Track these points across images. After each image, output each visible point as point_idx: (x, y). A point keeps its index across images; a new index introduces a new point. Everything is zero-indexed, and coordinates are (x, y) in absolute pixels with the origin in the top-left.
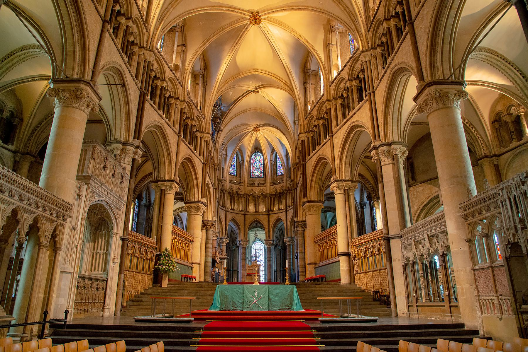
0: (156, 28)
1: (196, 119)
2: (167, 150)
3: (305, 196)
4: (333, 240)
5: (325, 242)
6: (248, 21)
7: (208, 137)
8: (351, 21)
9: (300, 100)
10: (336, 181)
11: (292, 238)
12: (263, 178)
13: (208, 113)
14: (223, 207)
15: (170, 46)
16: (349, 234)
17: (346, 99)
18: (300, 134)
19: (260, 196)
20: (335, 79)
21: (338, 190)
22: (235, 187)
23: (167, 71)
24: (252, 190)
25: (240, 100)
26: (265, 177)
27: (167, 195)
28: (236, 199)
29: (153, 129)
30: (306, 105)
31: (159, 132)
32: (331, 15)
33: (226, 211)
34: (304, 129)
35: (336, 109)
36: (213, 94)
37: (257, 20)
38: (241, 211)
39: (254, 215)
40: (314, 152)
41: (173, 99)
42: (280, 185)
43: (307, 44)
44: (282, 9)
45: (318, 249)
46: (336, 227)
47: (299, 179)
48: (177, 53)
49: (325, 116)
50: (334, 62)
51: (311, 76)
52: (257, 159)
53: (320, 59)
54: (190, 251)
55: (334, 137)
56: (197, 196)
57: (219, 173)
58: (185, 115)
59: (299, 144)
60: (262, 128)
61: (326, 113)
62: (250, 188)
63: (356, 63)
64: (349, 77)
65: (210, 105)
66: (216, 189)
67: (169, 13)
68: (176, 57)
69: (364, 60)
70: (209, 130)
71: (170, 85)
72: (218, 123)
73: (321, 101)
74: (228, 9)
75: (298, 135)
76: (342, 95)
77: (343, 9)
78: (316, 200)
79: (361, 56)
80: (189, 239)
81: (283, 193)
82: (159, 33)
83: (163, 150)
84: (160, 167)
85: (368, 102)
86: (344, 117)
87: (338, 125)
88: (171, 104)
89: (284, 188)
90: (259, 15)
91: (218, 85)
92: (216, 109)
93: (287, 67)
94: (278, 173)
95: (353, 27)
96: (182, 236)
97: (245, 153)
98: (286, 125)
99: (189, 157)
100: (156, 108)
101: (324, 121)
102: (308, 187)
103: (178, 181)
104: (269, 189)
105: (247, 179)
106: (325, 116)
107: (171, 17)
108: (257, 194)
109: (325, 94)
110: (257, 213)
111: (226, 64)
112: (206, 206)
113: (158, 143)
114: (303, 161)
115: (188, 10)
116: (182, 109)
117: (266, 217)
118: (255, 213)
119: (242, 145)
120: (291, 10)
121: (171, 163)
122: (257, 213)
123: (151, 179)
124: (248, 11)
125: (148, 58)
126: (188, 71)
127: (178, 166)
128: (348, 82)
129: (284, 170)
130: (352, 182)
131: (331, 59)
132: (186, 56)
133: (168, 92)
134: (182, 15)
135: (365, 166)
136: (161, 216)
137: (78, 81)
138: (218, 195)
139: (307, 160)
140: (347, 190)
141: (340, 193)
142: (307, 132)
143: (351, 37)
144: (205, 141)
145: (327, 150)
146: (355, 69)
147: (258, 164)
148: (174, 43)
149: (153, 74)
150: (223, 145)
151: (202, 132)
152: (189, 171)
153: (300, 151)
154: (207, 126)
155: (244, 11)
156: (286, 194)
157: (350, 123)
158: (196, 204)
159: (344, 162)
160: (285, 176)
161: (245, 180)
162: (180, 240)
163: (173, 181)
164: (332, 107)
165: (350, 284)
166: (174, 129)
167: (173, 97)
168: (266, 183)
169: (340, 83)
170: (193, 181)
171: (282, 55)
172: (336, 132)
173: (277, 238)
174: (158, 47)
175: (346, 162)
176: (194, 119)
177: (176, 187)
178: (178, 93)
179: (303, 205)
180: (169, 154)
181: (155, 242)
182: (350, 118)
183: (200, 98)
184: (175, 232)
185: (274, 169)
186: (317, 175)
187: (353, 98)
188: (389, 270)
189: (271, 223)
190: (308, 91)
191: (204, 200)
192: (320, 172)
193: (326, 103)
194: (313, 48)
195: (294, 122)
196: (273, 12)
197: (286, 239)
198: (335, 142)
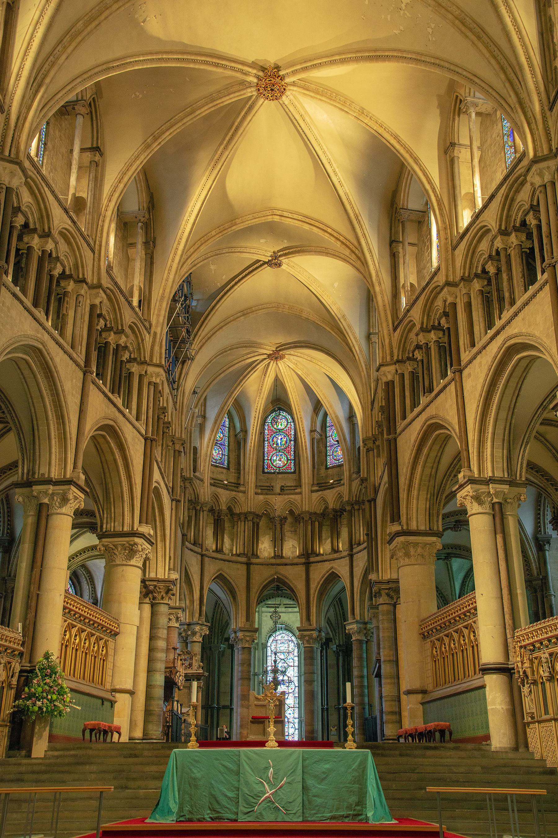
0: (25, 105)
2: (55, 406)
3: (396, 519)
4: (466, 632)
5: (447, 636)
6: (253, 89)
7: (158, 375)
8: (507, 85)
9: (380, 284)
10: (472, 481)
11: (366, 623)
12: (294, 472)
13: (158, 316)
14: (194, 544)
15: (64, 150)
16: (507, 616)
17: (493, 282)
18: (381, 366)
19: (286, 518)
20: (467, 230)
21: (475, 505)
22: (224, 496)
23: (57, 213)
24: (267, 503)
25: (236, 284)
26: (298, 471)
27: (55, 517)
28: (227, 525)
29: (21, 355)
30: (395, 295)
31: (34, 362)
32: (457, 69)
33: (202, 556)
34: (392, 356)
35: (469, 306)
36: (170, 270)
37: (276, 88)
38: (238, 555)
39: (272, 565)
40: (417, 410)
41: (72, 282)
42: (334, 490)
43: (398, 146)
44: (337, 57)
45: (429, 652)
46: (474, 598)
47: (381, 477)
48: (80, 168)
49: (443, 321)
50: (463, 189)
51: (408, 225)
52: (280, 427)
53: (430, 182)
54: (110, 658)
55: (465, 373)
57: (185, 462)
58: (102, 322)
59: (380, 391)
60: (292, 351)
61: (446, 314)
62: (261, 497)
63: (518, 191)
64: (500, 225)
65: (163, 297)
66: (178, 501)
67: (56, 68)
68: (78, 179)
69: (537, 181)
70: (161, 358)
71: (63, 247)
72: (183, 341)
73: (431, 286)
74: (203, 58)
75: (378, 370)
76: (484, 271)
77: (487, 55)
78: (422, 528)
79: (531, 174)
80: (108, 628)
81: (342, 510)
82: (34, 117)
83: (45, 406)
84: (37, 447)
85: (547, 288)
86: (490, 324)
87: (473, 345)
88: (65, 294)
89: (346, 498)
90: (281, 73)
91: (181, 247)
92: (179, 305)
93: (350, 203)
94: (330, 461)
95: (513, 99)
96: (90, 620)
97: (249, 411)
98: (348, 344)
99: (111, 423)
100: (29, 304)
101: (441, 336)
102: (403, 495)
103: (82, 482)
105: (254, 477)
106: (443, 321)
107: (63, 78)
108: (278, 513)
109: (443, 267)
110: (278, 561)
111: (202, 197)
112: (151, 543)
113: (34, 389)
114: (389, 433)
115: (104, 59)
116: (93, 307)
117: (301, 569)
118: (273, 561)
119: (243, 394)
120: (357, 60)
121: (65, 438)
122: (278, 561)
123: (14, 479)
124: (253, 65)
126: (109, 213)
127: (84, 445)
128: (499, 238)
129: (343, 453)
130: (512, 483)
131: (457, 182)
132: (103, 176)
133: (59, 265)
134: (89, 74)
135: (545, 445)
136: (37, 571)
138: (183, 515)
139: (398, 431)
140: (500, 504)
141: (481, 510)
142: (398, 361)
143: (507, 124)
144: (150, 383)
145: (448, 406)
146: (516, 206)
147: (280, 440)
148: (72, 144)
149: (20, 220)
150: (195, 392)
151: (144, 363)
152: (109, 457)
153: (381, 407)
154: (157, 348)
155: (243, 63)
156: (351, 513)
157: (502, 338)
158: (127, 539)
159: (490, 436)
160: (346, 468)
162: (83, 631)
163: (69, 482)
164: (458, 300)
166: (75, 355)
167: (70, 277)
168: (299, 486)
169: (479, 241)
170: (121, 482)
171: (336, 174)
172: (470, 362)
173: (329, 621)
174: (33, 153)
175: (494, 434)
176: (123, 331)
177: (76, 498)
178: (83, 267)
179: (390, 542)
180: (61, 418)
181: (20, 637)
182: (503, 328)
183: (138, 280)
184: (71, 610)
185: (320, 452)
186: (424, 467)
187: (510, 278)
189: (314, 586)
190: (401, 261)
191: (146, 529)
192: (430, 460)
193: (445, 290)
194: (411, 155)
195: (368, 337)
196: (314, 66)
197: (352, 627)
198: (468, 385)
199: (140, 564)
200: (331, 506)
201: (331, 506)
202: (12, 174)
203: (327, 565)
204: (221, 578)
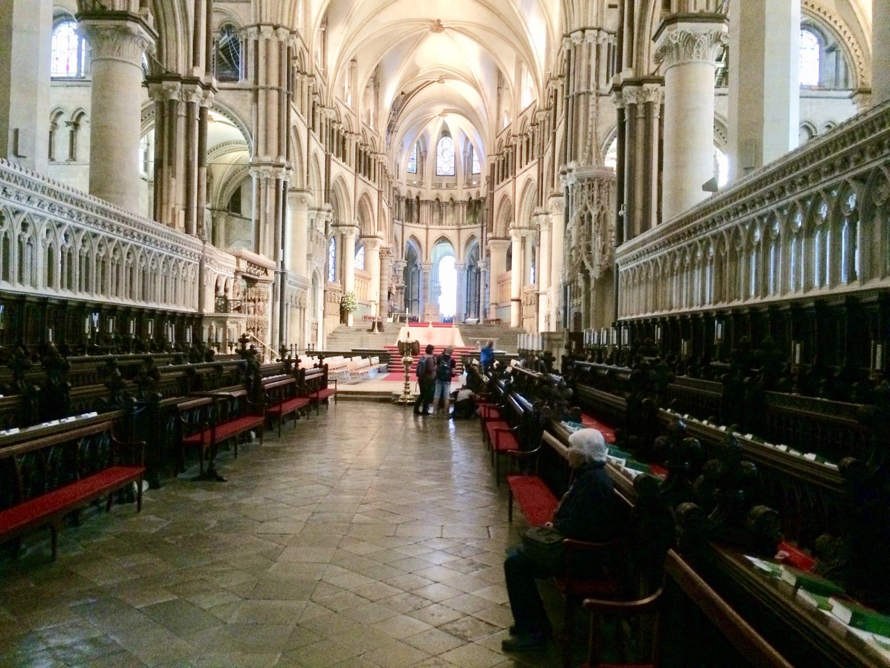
10: (514, 228)
14: (398, 220)
24: (438, 194)
26: (455, 175)
28: (415, 206)
40: (501, 184)
56: (372, 230)
62: (435, 191)
78: (502, 236)
87: (521, 167)
89: (481, 196)
103: (358, 225)
104: (461, 195)
116: (357, 144)
125: (329, 117)
142: (497, 155)
151: (376, 153)
154: (382, 144)
163: (353, 226)
165: (519, 326)
168: (456, 184)
176: (367, 145)
188: (536, 319)
197: (480, 264)
199: (379, 249)
200: (474, 198)
201: (474, 198)
203: (470, 231)
204: (413, 237)
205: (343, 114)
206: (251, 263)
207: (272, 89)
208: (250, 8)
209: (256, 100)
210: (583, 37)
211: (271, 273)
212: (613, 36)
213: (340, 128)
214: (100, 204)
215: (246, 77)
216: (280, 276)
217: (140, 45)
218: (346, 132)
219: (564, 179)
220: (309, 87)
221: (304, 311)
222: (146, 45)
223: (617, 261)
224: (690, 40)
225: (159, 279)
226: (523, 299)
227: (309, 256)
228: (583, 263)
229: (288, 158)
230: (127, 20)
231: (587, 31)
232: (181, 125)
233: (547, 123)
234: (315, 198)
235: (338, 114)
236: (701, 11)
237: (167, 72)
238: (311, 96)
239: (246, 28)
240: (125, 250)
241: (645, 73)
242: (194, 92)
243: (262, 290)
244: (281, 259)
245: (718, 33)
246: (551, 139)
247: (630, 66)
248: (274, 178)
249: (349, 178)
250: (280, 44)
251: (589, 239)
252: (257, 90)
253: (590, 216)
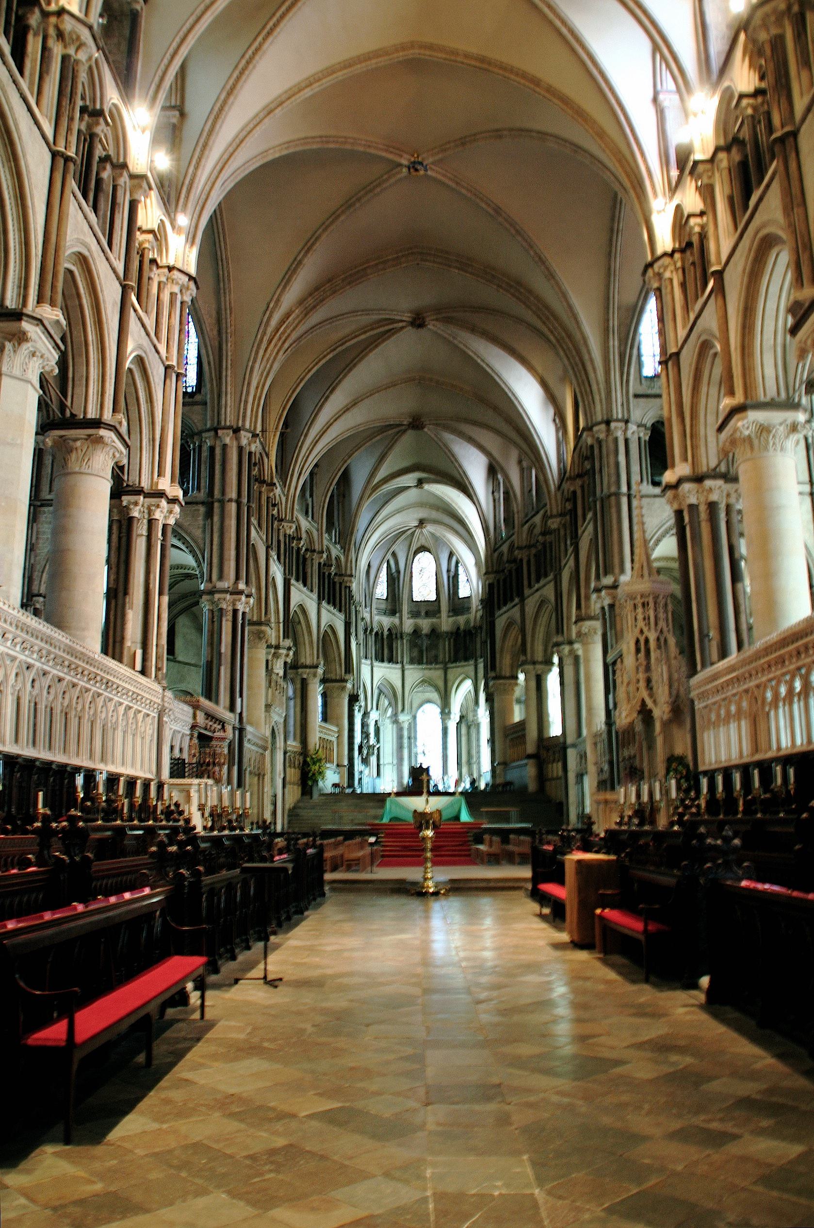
1: (334, 562)
40: (504, 609)
78: (508, 674)
89: (472, 624)
102: (498, 656)
104: (446, 623)
116: (320, 564)
125: (288, 532)
137: (259, 623)
151: (341, 575)
161: (405, 608)
172: (529, 597)
180: (310, 632)
188: (563, 781)
198: (527, 609)
200: (462, 627)
201: (462, 627)
202: (291, 528)
205: (303, 530)
206: (209, 716)
207: (230, 500)
208: (206, 410)
209: (209, 515)
210: (608, 430)
211: (229, 729)
212: (643, 429)
213: (300, 546)
214: (68, 641)
215: (199, 489)
216: (237, 732)
217: (111, 455)
218: (307, 550)
219: (599, 597)
220: (268, 498)
221: (263, 779)
222: (117, 455)
223: (693, 694)
224: (764, 430)
225: (119, 734)
226: (543, 753)
227: (268, 707)
228: (643, 701)
229: (247, 583)
230: (99, 428)
231: (613, 425)
232: (140, 546)
233: (562, 533)
234: (272, 634)
235: (298, 528)
236: (772, 399)
237: (128, 485)
238: (271, 508)
239: (200, 433)
240: (89, 697)
241: (705, 469)
242: (158, 506)
243: (218, 750)
244: (238, 710)
245: (794, 423)
246: (570, 550)
247: (686, 460)
248: (230, 608)
249: (312, 606)
250: (240, 449)
251: (648, 668)
252: (212, 503)
253: (647, 641)
